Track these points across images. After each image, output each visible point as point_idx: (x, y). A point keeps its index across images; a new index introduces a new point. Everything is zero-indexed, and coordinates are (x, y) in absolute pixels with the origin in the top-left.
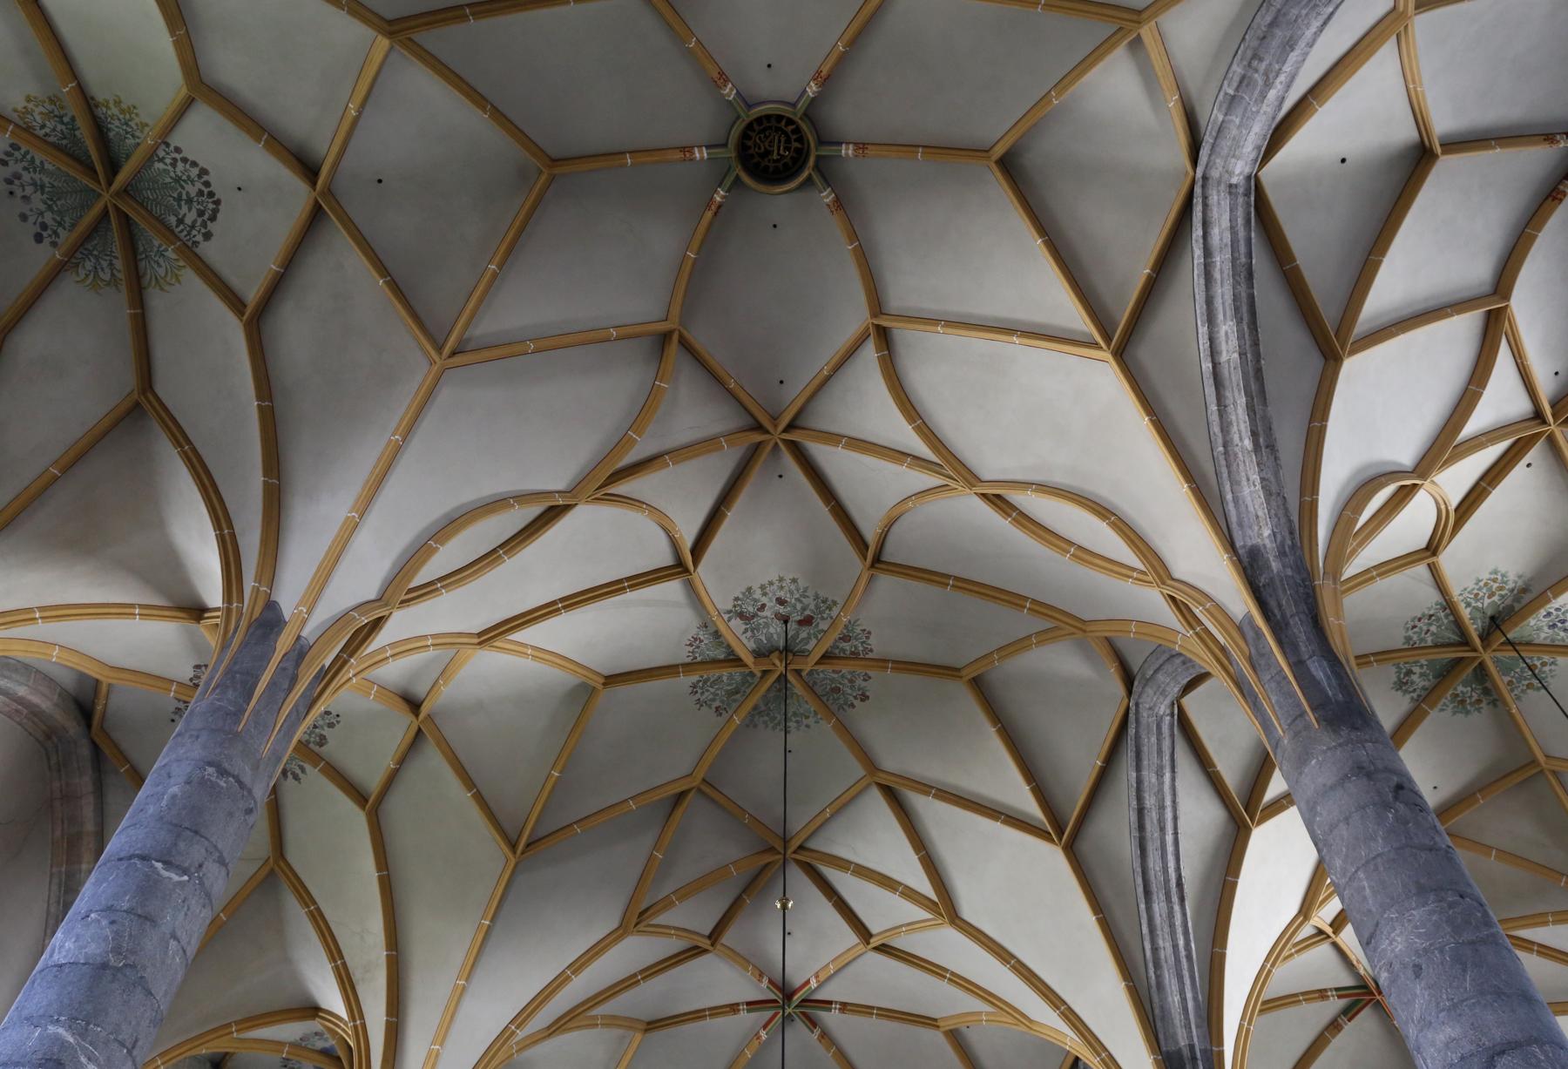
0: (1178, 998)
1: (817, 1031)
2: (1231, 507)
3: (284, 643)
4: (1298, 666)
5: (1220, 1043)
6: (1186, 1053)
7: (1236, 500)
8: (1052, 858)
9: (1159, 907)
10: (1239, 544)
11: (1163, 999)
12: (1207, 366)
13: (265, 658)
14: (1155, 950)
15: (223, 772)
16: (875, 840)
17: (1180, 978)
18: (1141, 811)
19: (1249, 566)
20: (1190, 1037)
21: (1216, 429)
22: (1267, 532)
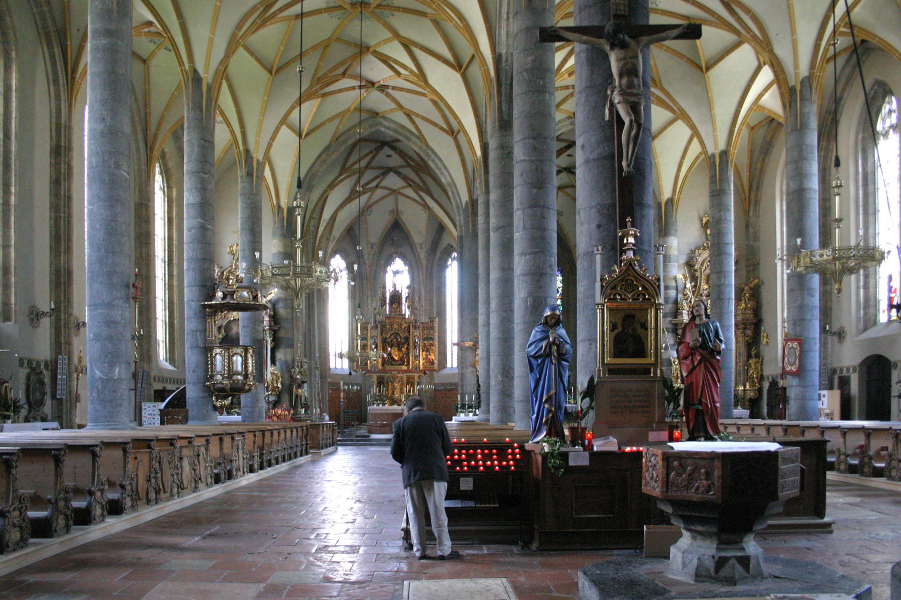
3: (204, 88)
4: (500, 103)
8: (457, 76)
13: (201, 95)
15: (205, 141)
19: (498, 59)
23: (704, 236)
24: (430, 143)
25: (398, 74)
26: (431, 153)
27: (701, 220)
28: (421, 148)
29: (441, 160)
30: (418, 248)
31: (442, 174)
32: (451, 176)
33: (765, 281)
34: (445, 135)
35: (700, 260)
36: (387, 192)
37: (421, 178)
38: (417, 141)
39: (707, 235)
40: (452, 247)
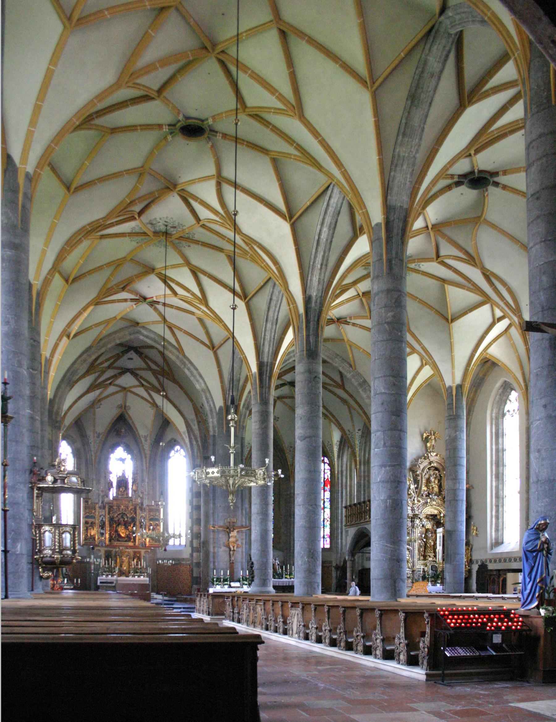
0: (267, 349)
1: (153, 307)
2: (309, 281)
5: (276, 360)
6: (266, 363)
7: (311, 280)
9: (269, 325)
10: (307, 293)
11: (263, 348)
12: (317, 237)
14: (265, 335)
16: (185, 277)
17: (270, 345)
18: (271, 299)
19: (307, 300)
20: (268, 359)
21: (313, 257)
22: (315, 294)
23: (424, 449)
24: (187, 354)
25: (175, 293)
26: (187, 362)
27: (422, 436)
28: (178, 357)
29: (196, 369)
30: (143, 439)
31: (197, 381)
32: (205, 384)
33: (474, 486)
34: (205, 348)
35: (422, 467)
36: (118, 389)
37: (158, 380)
38: (175, 351)
39: (426, 446)
40: (175, 441)
